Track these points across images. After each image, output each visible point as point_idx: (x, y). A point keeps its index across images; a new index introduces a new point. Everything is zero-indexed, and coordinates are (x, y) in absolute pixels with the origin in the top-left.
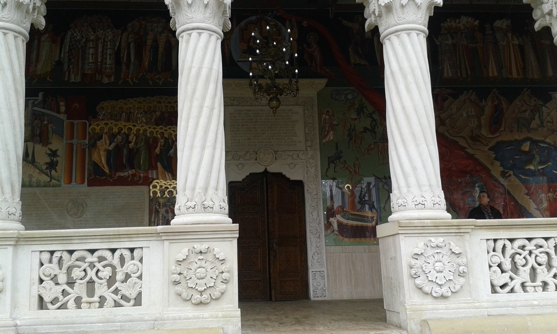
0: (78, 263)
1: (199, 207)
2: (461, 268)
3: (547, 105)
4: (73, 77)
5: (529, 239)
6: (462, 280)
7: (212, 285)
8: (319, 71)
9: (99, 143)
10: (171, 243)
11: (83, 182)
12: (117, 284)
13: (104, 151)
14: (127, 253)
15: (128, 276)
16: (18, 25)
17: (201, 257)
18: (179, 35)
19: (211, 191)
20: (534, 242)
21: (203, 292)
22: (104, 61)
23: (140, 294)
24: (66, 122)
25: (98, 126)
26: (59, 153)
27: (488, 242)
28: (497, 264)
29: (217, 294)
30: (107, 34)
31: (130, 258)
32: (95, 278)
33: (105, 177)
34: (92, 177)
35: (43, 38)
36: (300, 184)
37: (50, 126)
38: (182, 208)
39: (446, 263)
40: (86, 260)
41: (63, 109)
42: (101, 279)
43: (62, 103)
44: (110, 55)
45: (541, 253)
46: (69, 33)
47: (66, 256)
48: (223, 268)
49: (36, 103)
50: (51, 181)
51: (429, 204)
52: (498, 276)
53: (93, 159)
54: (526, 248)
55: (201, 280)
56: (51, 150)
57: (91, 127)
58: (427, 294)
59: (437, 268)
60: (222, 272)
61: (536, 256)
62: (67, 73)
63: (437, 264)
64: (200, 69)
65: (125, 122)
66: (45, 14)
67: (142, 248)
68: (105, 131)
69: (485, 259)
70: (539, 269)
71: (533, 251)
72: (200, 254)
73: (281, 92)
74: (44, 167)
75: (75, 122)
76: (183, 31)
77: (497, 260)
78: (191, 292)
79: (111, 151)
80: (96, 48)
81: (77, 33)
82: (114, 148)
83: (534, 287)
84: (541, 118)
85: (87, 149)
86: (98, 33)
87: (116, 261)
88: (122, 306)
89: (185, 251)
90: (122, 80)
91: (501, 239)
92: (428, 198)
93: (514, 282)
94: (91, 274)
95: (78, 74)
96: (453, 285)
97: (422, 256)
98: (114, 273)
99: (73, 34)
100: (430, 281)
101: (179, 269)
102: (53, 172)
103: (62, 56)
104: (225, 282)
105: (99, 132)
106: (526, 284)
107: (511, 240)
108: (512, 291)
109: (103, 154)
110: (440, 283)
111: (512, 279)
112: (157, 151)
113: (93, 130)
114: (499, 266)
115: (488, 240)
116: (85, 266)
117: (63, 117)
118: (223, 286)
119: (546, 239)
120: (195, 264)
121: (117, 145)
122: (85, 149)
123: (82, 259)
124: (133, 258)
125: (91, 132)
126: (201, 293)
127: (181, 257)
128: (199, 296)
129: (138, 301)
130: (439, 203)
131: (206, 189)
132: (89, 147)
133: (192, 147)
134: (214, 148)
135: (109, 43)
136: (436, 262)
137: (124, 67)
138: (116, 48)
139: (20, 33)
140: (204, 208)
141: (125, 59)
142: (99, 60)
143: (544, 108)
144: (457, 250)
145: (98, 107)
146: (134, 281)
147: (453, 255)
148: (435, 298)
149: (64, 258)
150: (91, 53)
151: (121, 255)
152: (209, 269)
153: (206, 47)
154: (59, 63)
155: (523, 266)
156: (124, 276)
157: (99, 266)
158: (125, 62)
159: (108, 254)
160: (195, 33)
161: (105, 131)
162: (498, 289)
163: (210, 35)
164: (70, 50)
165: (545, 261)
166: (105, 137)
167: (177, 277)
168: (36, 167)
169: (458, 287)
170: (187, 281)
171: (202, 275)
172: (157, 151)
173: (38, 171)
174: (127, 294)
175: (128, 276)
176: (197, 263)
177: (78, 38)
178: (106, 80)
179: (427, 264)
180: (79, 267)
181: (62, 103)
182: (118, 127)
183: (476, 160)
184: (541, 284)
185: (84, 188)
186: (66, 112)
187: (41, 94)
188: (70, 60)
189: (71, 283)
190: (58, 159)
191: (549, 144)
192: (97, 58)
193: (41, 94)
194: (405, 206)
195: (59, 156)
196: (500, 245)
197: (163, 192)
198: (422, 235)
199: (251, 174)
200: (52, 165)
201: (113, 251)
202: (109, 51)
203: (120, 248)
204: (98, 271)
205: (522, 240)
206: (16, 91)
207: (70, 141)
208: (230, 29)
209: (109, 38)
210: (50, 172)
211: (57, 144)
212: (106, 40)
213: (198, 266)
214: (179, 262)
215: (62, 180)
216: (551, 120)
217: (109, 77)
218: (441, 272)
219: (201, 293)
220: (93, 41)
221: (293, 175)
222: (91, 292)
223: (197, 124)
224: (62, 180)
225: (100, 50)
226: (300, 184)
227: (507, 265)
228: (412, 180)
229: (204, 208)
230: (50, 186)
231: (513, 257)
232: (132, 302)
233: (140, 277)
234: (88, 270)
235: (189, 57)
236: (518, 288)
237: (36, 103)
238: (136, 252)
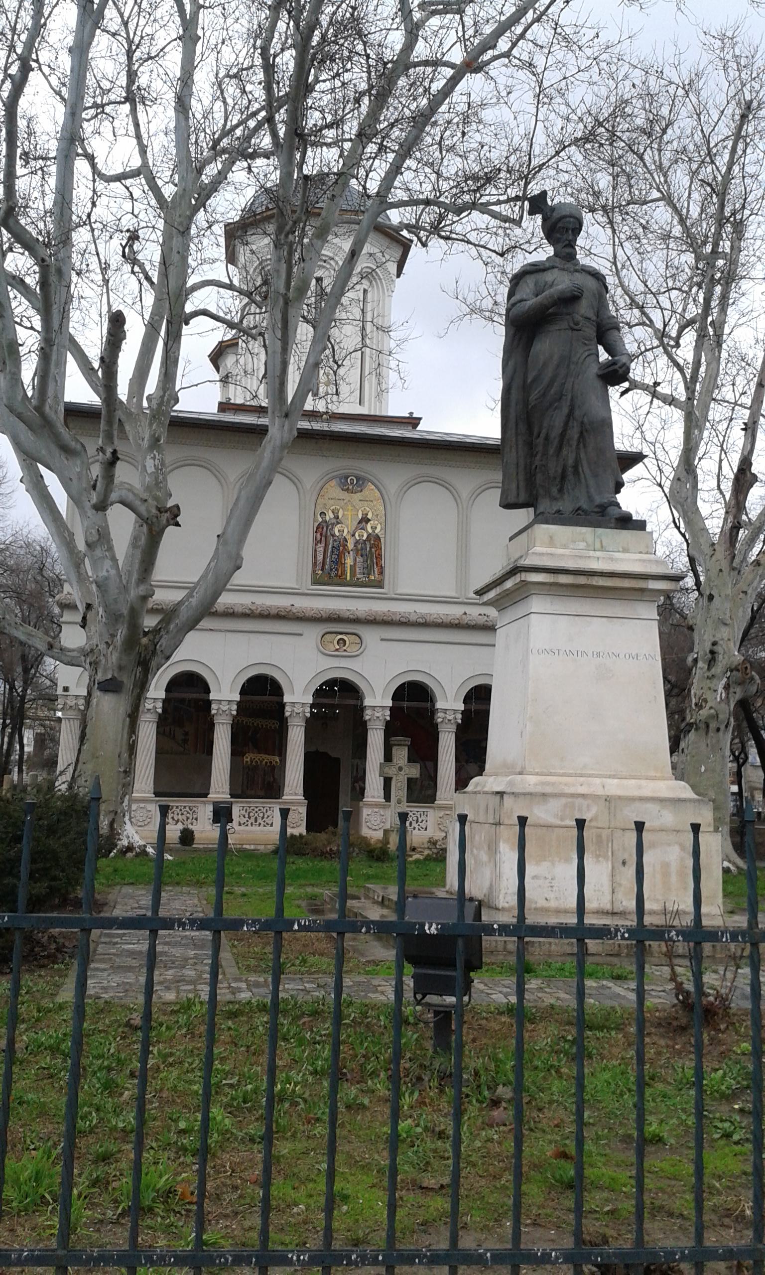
36: (337, 760)
129: (272, 825)
189: (249, 818)
197: (252, 762)
200: (185, 741)
221: (334, 754)
222: (256, 821)
226: (337, 760)
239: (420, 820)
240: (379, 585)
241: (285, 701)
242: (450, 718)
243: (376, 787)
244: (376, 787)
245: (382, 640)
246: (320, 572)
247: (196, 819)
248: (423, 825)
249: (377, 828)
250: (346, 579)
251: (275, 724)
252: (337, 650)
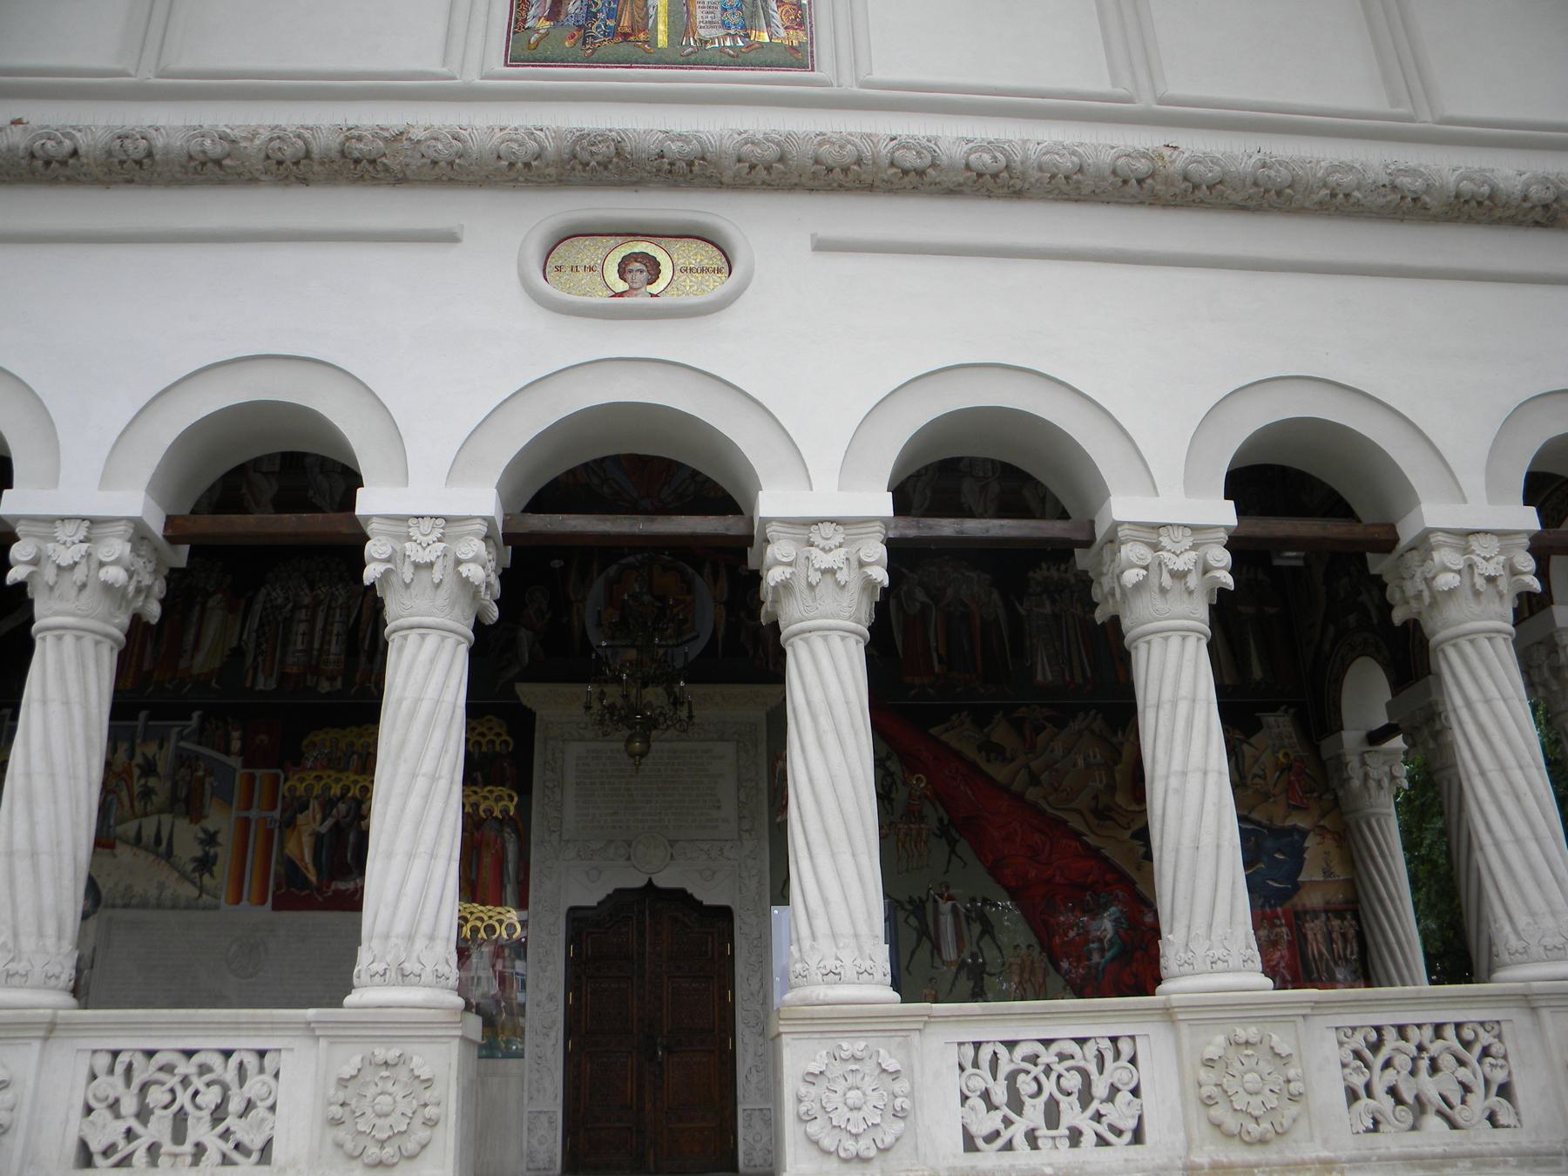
0: (161, 1076)
1: (391, 975)
2: (898, 1102)
3: (1253, 740)
4: (261, 679)
5: (1046, 1043)
6: (899, 1126)
7: (403, 1128)
8: (771, 667)
9: (301, 818)
10: (332, 1043)
11: (263, 902)
12: (230, 1122)
13: (310, 835)
14: (251, 1061)
15: (250, 1105)
16: (105, 621)
17: (385, 1073)
18: (389, 637)
19: (420, 944)
20: (1055, 1048)
21: (385, 1141)
22: (326, 647)
23: (269, 1141)
24: (241, 772)
25: (302, 782)
26: (220, 838)
27: (962, 1047)
28: (979, 1093)
29: (411, 1146)
30: (337, 593)
31: (256, 1069)
32: (189, 1107)
33: (307, 892)
34: (283, 891)
35: (211, 603)
37: (208, 780)
38: (363, 975)
39: (869, 1092)
40: (176, 1071)
42: (199, 1108)
43: (236, 734)
44: (338, 635)
45: (1068, 1070)
46: (263, 591)
47: (138, 1061)
48: (427, 1096)
49: (186, 732)
50: (200, 896)
51: (849, 972)
52: (980, 1116)
53: (287, 851)
54: (1039, 1060)
55: (383, 1119)
56: (205, 831)
57: (286, 786)
58: (827, 1153)
59: (850, 1102)
60: (425, 1105)
61: (1059, 1076)
62: (251, 673)
63: (851, 1094)
64: (418, 701)
65: (356, 773)
66: (162, 596)
67: (279, 1050)
68: (315, 793)
69: (953, 1082)
70: (1064, 1102)
71: (1053, 1066)
72: (384, 1067)
73: (651, 724)
74: (190, 867)
75: (259, 773)
76: (394, 631)
77: (978, 1084)
78: (363, 1141)
79: (323, 835)
80: (312, 622)
81: (278, 591)
82: (331, 830)
83: (1053, 1138)
84: (1241, 767)
85: (277, 832)
86: (319, 592)
87: (230, 1076)
88: (233, 1163)
89: (356, 1061)
90: (356, 687)
91: (988, 1042)
92: (848, 962)
93: (1012, 1129)
94: (183, 1098)
95: (271, 675)
96: (881, 1135)
97: (822, 1077)
98: (225, 1099)
99: (269, 594)
100: (834, 1127)
101: (341, 1096)
102: (206, 877)
103: (245, 637)
104: (431, 1123)
105: (304, 794)
106: (1038, 1133)
107: (1011, 1045)
108: (1009, 1146)
109: (307, 841)
110: (853, 1131)
111: (1008, 1122)
113: (292, 789)
114: (986, 1095)
115: (960, 1044)
116: (173, 1081)
117: (235, 762)
118: (422, 1134)
119: (1082, 1041)
120: (374, 1087)
121: (337, 824)
122: (272, 831)
123: (168, 1069)
124: (262, 1070)
125: (287, 794)
126: (382, 1144)
127: (348, 1071)
128: (376, 1150)
130: (870, 971)
131: (410, 938)
132: (280, 827)
133: (389, 855)
134: (433, 856)
135: (338, 610)
136: (850, 1089)
137: (363, 659)
138: (352, 621)
139: (107, 636)
140: (403, 975)
141: (367, 642)
142: (316, 645)
143: (1245, 747)
144: (891, 1064)
145: (305, 742)
146: (260, 1115)
147: (884, 1076)
148: (846, 1161)
149: (135, 1065)
150: (301, 631)
151: (241, 1064)
152: (399, 1098)
153: (432, 661)
154: (238, 653)
155: (1032, 1096)
156: (243, 1105)
157: (198, 1083)
158: (366, 648)
159: (216, 1061)
160: (413, 636)
161: (315, 793)
162: (980, 1143)
163: (443, 639)
164: (261, 625)
165: (1075, 1086)
166: (314, 805)
167: (337, 1111)
168: (174, 867)
169: (889, 1140)
170: (357, 1120)
171: (386, 1109)
173: (177, 875)
174: (246, 1139)
175: (250, 1105)
176: (376, 1085)
177: (279, 601)
178: (325, 687)
179: (832, 1095)
180: (162, 1084)
181: (236, 734)
182: (341, 784)
183: (1106, 859)
184: (1067, 1132)
185: (265, 912)
186: (242, 753)
187: (196, 715)
188: (258, 645)
190: (219, 850)
191: (1259, 824)
192: (311, 642)
193: (196, 715)
194: (806, 976)
195: (219, 844)
196: (985, 1054)
198: (828, 1035)
199: (618, 891)
200: (205, 864)
201: (227, 1054)
202: (336, 628)
203: (240, 1050)
204: (196, 1093)
205: (1029, 1044)
206: (88, 741)
207: (245, 814)
208: (495, 619)
209: (340, 601)
210: (201, 876)
211: (220, 820)
212: (333, 604)
213: (379, 1090)
214: (343, 1083)
215: (223, 897)
216: (1261, 773)
217: (332, 679)
218: (859, 1109)
219: (382, 1144)
220: (306, 607)
221: (709, 896)
223: (403, 809)
224: (223, 897)
225: (319, 624)
227: (1000, 1094)
228: (821, 924)
229: (403, 975)
230: (197, 908)
231: (1012, 1077)
232: (255, 1157)
233: (272, 1108)
234: (179, 1089)
235: (399, 681)
236: (1020, 1141)
237: (186, 732)
238: (268, 1057)
239: (1100, 1088)
240: (798, 58)
241: (360, 510)
242: (1180, 564)
243: (843, 926)
244: (843, 926)
245: (822, 246)
246: (545, 25)
248: (1121, 1113)
249: (864, 1146)
250: (651, 41)
252: (621, 295)
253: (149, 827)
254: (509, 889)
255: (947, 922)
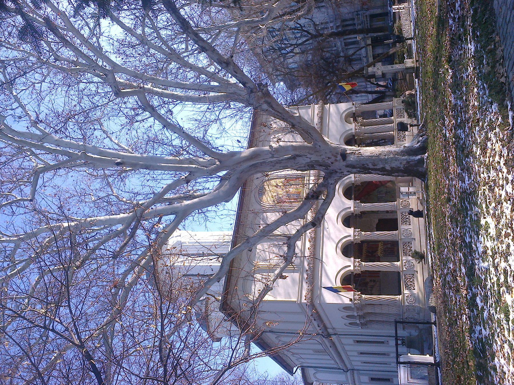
41: (357, 279)
112: (370, 255)
117: (360, 279)
172: (370, 255)
200: (374, 281)
221: (377, 221)
247: (409, 242)
251: (365, 246)
253: (369, 289)
254: (377, 243)
255: (380, 195)
